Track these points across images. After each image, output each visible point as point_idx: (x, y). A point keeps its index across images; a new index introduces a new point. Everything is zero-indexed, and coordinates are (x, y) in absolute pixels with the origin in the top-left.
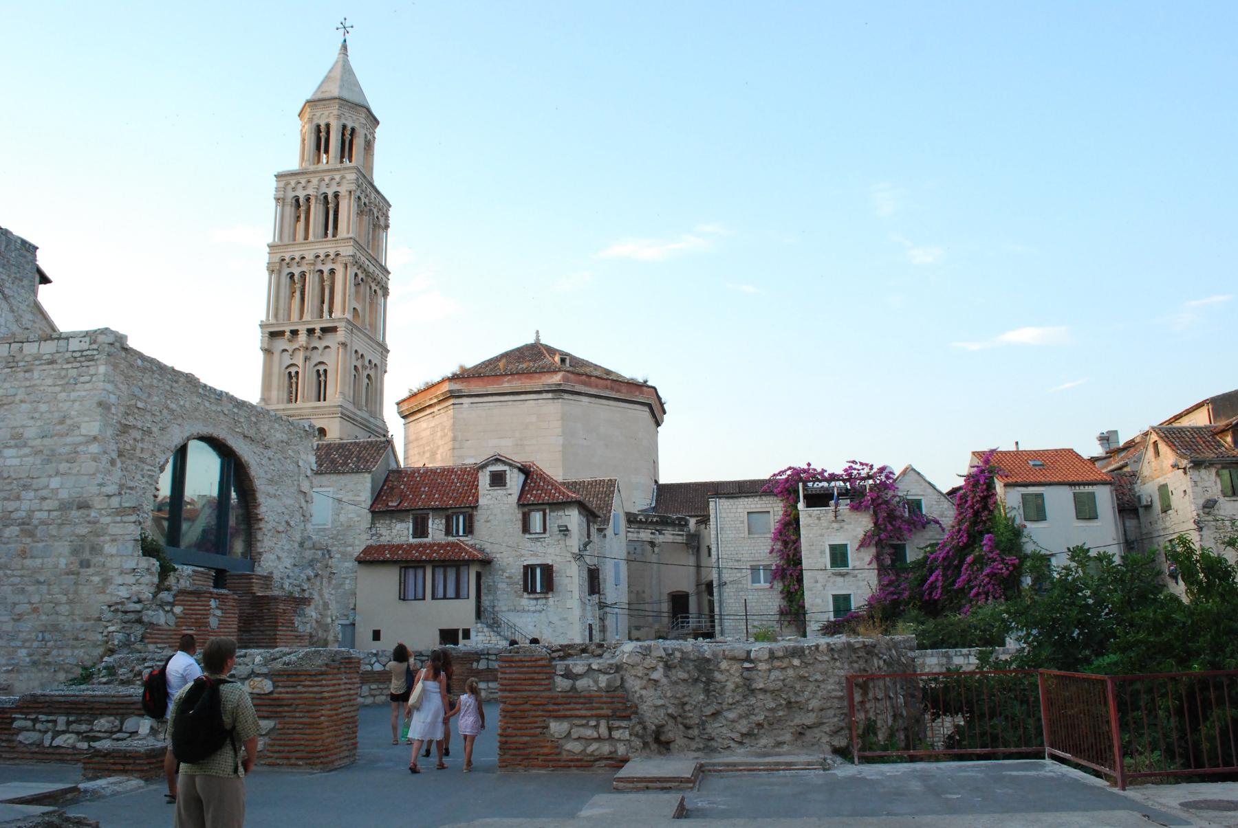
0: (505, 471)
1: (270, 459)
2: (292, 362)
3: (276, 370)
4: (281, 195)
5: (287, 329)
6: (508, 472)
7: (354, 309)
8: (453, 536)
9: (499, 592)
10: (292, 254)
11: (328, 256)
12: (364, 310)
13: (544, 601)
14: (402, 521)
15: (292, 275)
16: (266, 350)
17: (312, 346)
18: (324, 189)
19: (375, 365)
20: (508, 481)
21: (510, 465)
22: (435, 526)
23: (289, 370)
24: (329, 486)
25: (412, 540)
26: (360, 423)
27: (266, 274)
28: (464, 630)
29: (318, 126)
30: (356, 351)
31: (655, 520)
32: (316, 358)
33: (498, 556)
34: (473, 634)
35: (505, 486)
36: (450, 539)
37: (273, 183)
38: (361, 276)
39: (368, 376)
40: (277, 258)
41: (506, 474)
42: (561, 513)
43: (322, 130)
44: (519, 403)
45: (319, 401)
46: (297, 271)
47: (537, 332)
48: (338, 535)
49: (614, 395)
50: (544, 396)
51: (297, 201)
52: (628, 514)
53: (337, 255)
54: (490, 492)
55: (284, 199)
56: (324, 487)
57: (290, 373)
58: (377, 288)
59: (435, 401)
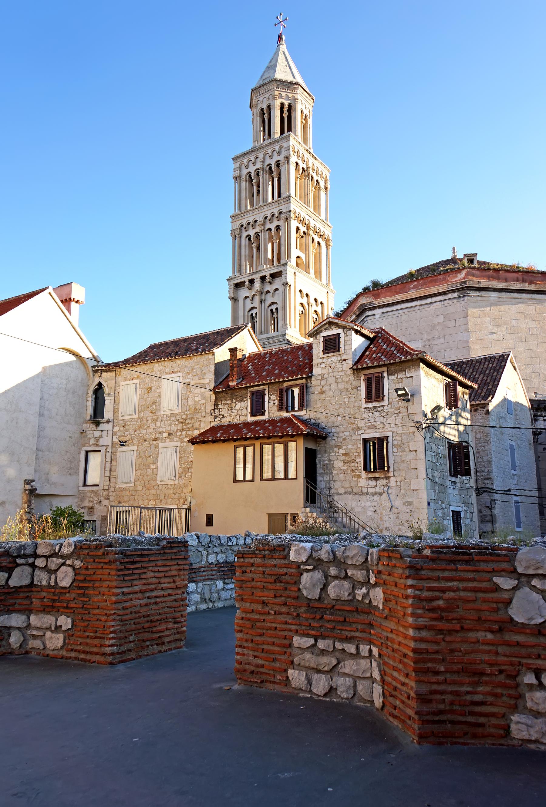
0: (339, 334)
4: (237, 173)
5: (246, 279)
6: (342, 335)
8: (288, 411)
9: (335, 472)
10: (247, 219)
11: (273, 215)
13: (384, 482)
14: (242, 401)
15: (249, 237)
16: (233, 298)
18: (268, 162)
19: (322, 303)
20: (342, 345)
21: (344, 328)
25: (250, 419)
27: (231, 239)
29: (262, 109)
30: (301, 291)
32: (269, 300)
33: (333, 430)
35: (339, 351)
36: (285, 414)
37: (232, 165)
38: (303, 229)
40: (237, 225)
41: (339, 338)
42: (401, 375)
43: (265, 112)
44: (426, 306)
46: (252, 232)
47: (454, 249)
48: (186, 419)
49: (526, 287)
50: (450, 296)
51: (250, 176)
53: (280, 213)
54: (324, 360)
55: (240, 177)
58: (320, 240)
59: (354, 317)
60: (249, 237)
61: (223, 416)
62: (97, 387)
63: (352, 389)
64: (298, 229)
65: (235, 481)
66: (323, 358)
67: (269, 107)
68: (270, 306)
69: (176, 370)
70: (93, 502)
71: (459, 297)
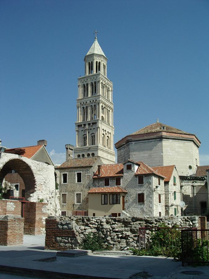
1: (38, 164)
2: (85, 134)
5: (83, 124)
6: (132, 165)
7: (102, 116)
14: (102, 181)
15: (84, 108)
17: (90, 128)
19: (110, 133)
22: (111, 182)
23: (84, 136)
26: (106, 151)
28: (119, 213)
30: (103, 129)
31: (194, 178)
34: (121, 215)
39: (108, 137)
45: (93, 145)
46: (85, 107)
50: (157, 140)
51: (84, 85)
60: (84, 108)
61: (96, 185)
63: (135, 180)
64: (102, 106)
65: (102, 204)
67: (92, 62)
68: (91, 134)
71: (160, 140)
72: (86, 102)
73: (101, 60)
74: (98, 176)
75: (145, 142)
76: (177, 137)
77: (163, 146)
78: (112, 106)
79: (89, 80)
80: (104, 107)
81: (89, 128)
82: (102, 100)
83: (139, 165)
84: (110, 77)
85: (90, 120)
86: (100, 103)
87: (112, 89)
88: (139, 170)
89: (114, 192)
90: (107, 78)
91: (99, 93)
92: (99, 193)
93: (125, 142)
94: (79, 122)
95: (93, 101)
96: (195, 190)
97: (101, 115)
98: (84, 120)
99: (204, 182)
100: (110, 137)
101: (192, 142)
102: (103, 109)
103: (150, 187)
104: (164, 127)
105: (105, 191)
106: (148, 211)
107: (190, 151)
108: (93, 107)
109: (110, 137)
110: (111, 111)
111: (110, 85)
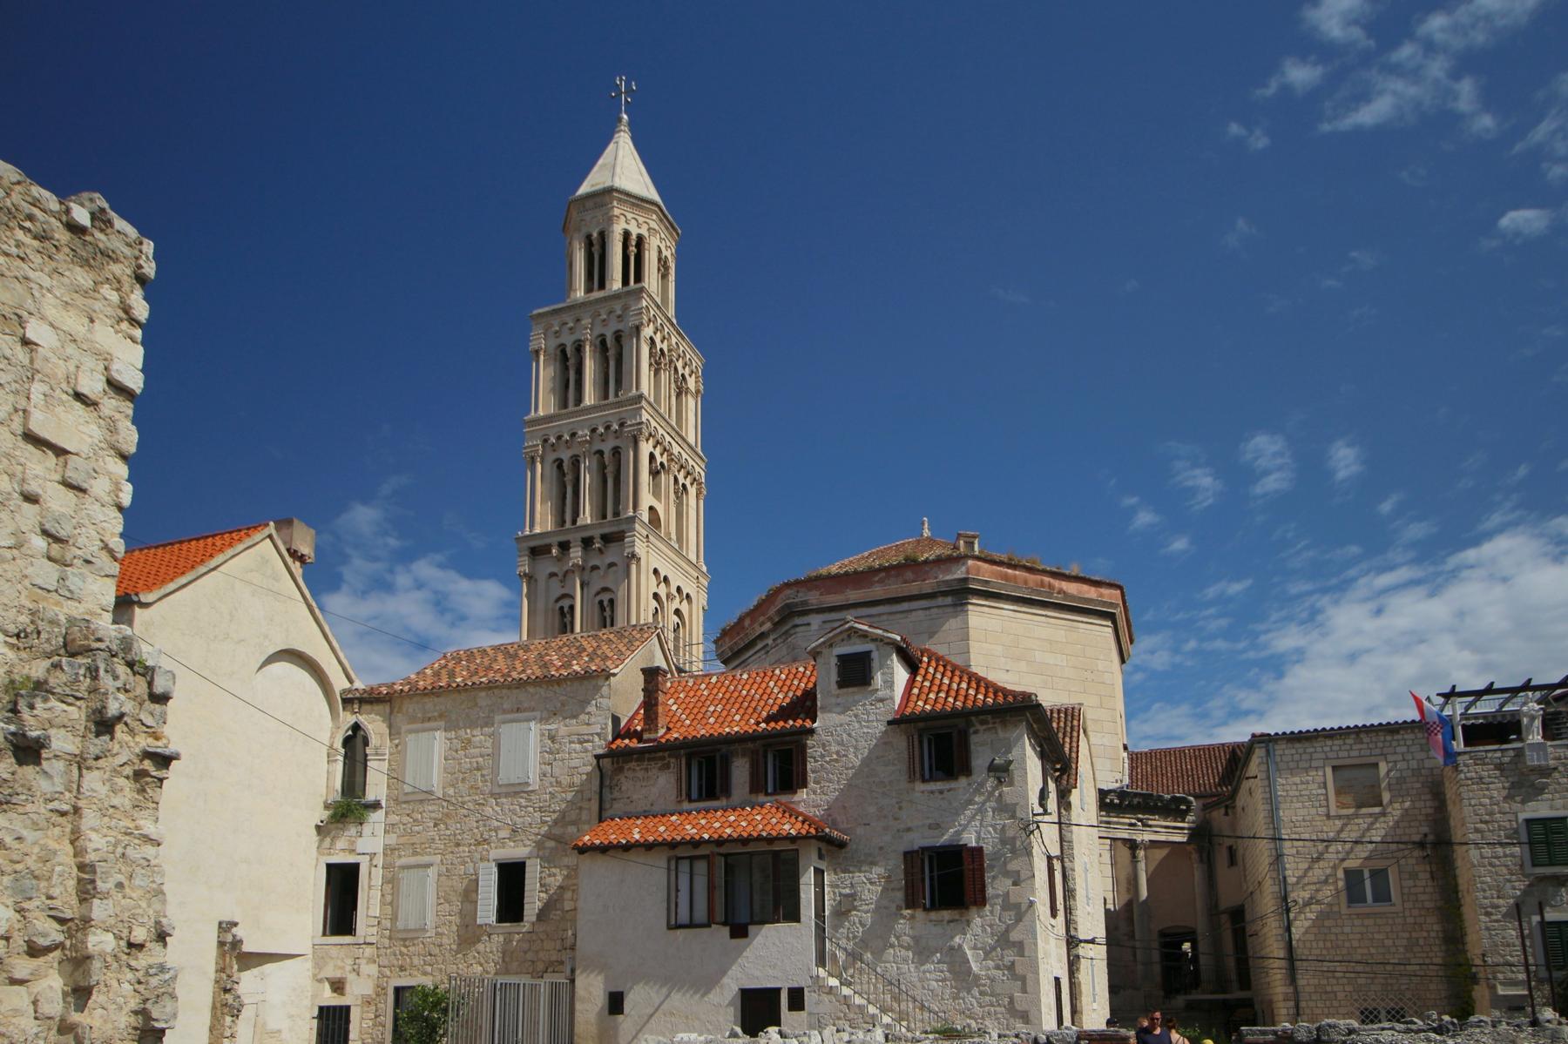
0: (869, 653)
3: (541, 605)
6: (875, 655)
7: (651, 508)
8: (767, 794)
12: (667, 510)
24: (533, 710)
46: (566, 455)
52: (1103, 794)
56: (525, 710)
57: (562, 608)
60: (559, 463)
62: (350, 733)
64: (652, 456)
66: (838, 696)
69: (526, 705)
70: (342, 968)
72: (573, 435)
73: (649, 229)
74: (646, 736)
75: (880, 615)
76: (1039, 593)
77: (972, 632)
78: (697, 469)
79: (586, 321)
80: (662, 464)
81: (584, 561)
82: (653, 424)
83: (912, 665)
84: (689, 320)
85: (589, 522)
86: (643, 438)
87: (701, 388)
88: (916, 691)
89: (760, 838)
90: (675, 321)
91: (637, 389)
92: (649, 847)
93: (770, 619)
94: (538, 530)
95: (608, 428)
96: (1142, 866)
97: (647, 499)
98: (561, 522)
99: (1186, 825)
100: (691, 615)
101: (1109, 623)
102: (655, 473)
103: (1009, 800)
104: (973, 543)
105: (691, 831)
106: (997, 967)
107: (1100, 668)
108: (607, 456)
109: (691, 615)
110: (692, 491)
111: (690, 362)
